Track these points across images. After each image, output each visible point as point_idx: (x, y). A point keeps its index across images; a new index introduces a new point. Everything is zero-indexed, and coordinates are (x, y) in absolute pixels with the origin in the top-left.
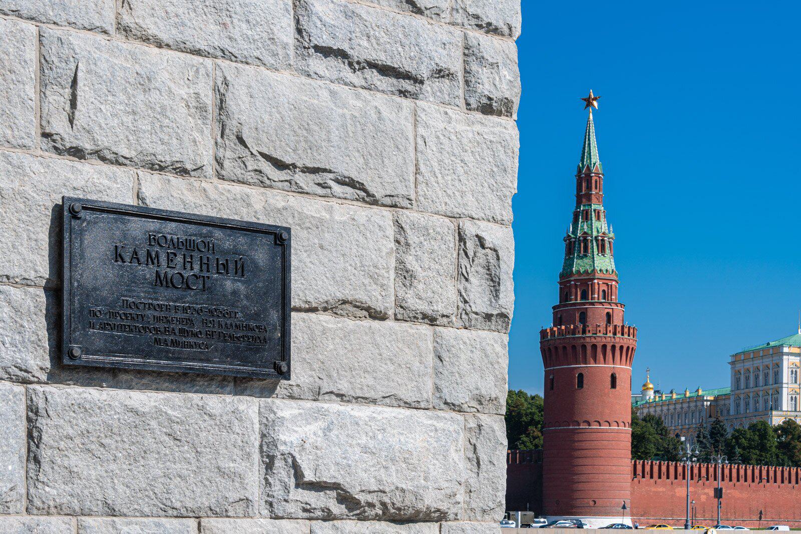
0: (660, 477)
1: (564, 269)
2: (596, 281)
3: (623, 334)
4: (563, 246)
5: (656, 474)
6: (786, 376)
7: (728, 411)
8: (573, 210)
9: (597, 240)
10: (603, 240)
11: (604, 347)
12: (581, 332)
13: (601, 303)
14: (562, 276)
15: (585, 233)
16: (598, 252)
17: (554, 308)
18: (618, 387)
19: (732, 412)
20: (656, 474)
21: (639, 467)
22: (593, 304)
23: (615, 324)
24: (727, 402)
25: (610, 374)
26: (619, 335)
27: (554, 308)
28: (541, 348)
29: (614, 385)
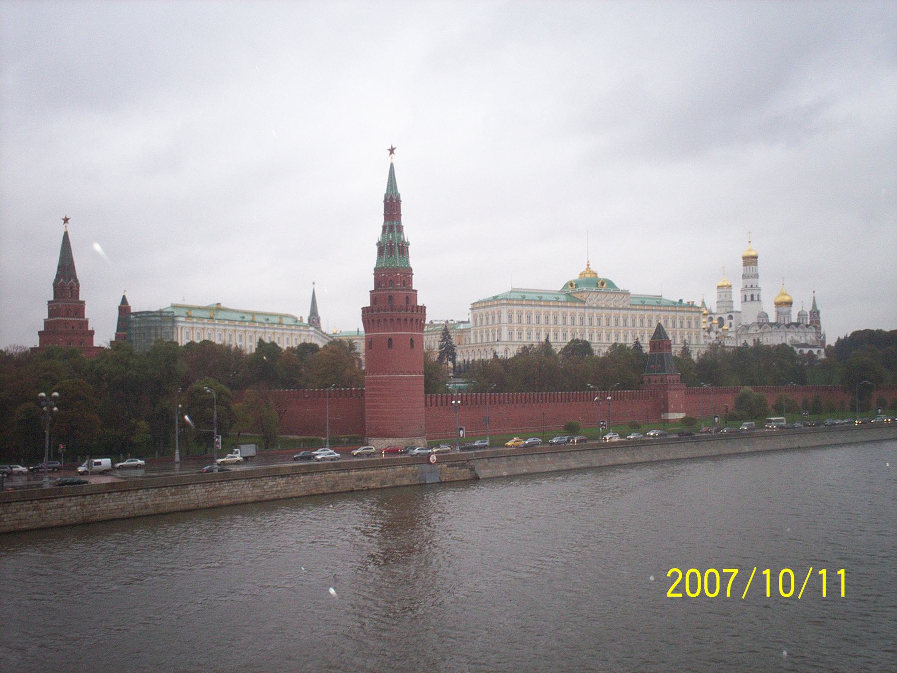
0: (442, 405)
1: (377, 265)
2: (398, 274)
3: (417, 311)
4: (376, 249)
5: (439, 404)
6: (505, 318)
7: (470, 339)
8: (382, 224)
9: (398, 246)
10: (402, 246)
11: (406, 319)
12: (390, 310)
13: (403, 290)
14: (375, 270)
15: (391, 241)
16: (399, 254)
17: (371, 292)
18: (415, 348)
19: (472, 341)
20: (439, 404)
21: (428, 399)
22: (396, 290)
23: (412, 304)
24: (469, 334)
25: (410, 339)
26: (415, 312)
27: (371, 292)
28: (363, 319)
29: (412, 347)
